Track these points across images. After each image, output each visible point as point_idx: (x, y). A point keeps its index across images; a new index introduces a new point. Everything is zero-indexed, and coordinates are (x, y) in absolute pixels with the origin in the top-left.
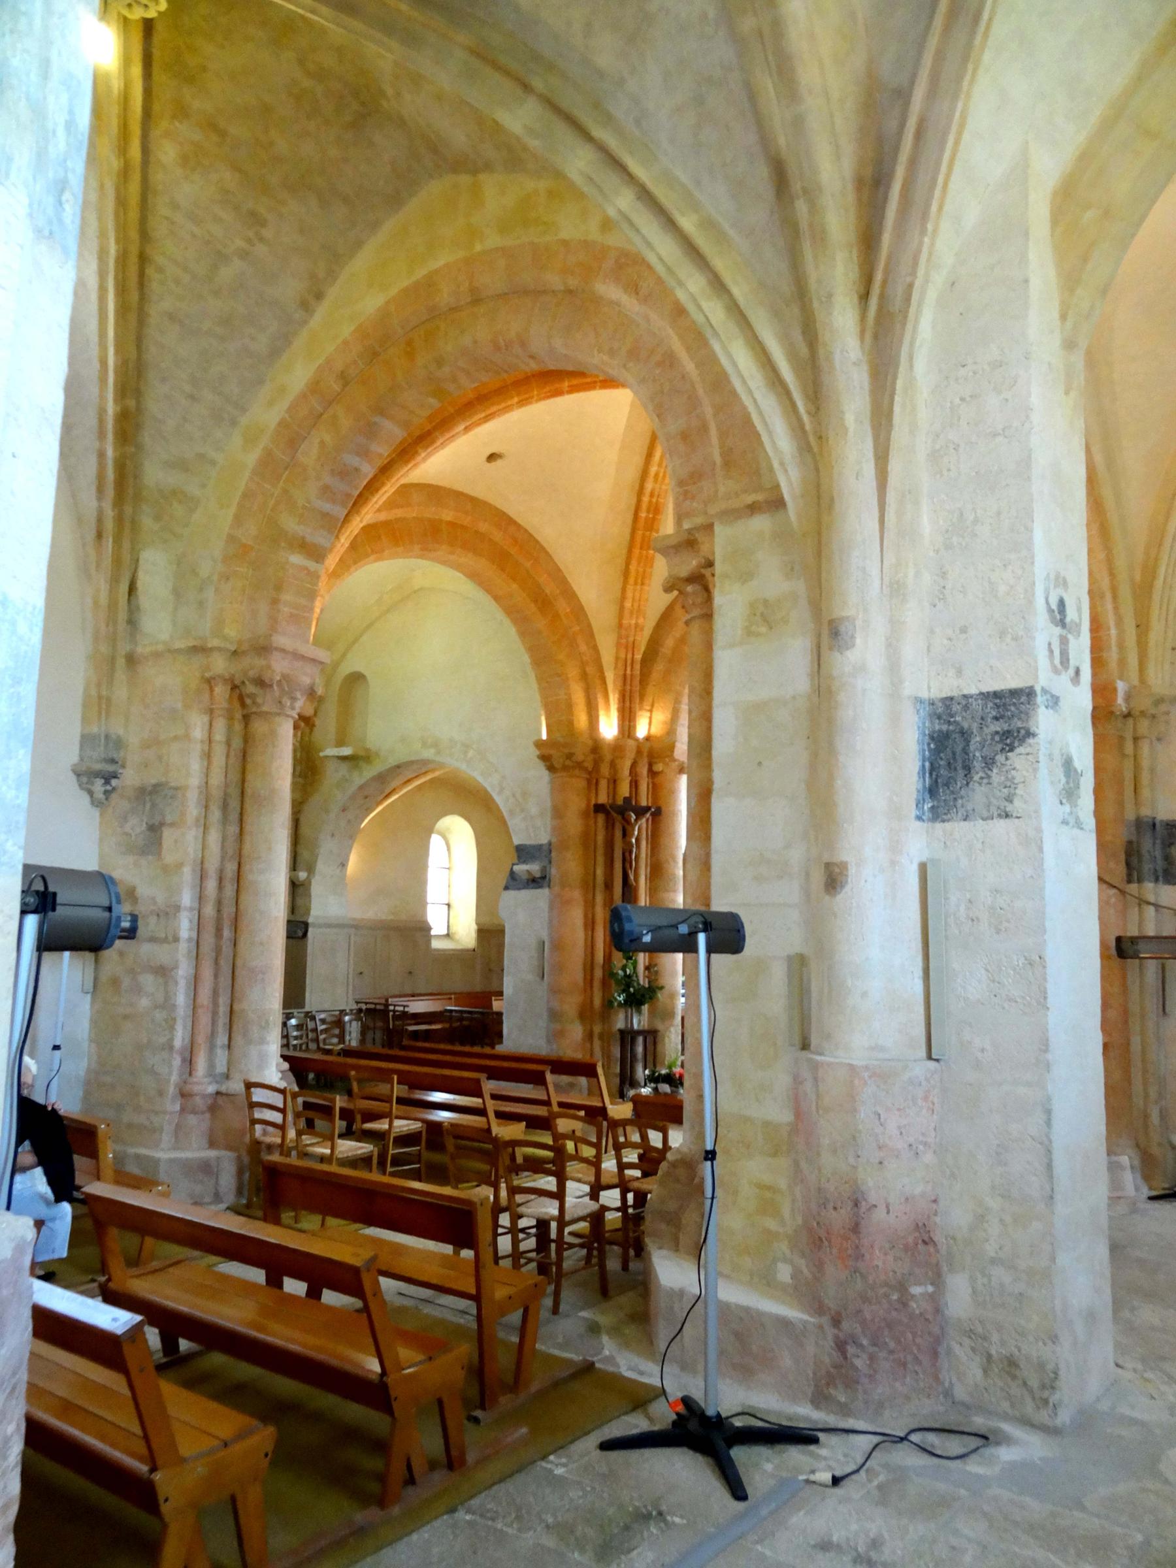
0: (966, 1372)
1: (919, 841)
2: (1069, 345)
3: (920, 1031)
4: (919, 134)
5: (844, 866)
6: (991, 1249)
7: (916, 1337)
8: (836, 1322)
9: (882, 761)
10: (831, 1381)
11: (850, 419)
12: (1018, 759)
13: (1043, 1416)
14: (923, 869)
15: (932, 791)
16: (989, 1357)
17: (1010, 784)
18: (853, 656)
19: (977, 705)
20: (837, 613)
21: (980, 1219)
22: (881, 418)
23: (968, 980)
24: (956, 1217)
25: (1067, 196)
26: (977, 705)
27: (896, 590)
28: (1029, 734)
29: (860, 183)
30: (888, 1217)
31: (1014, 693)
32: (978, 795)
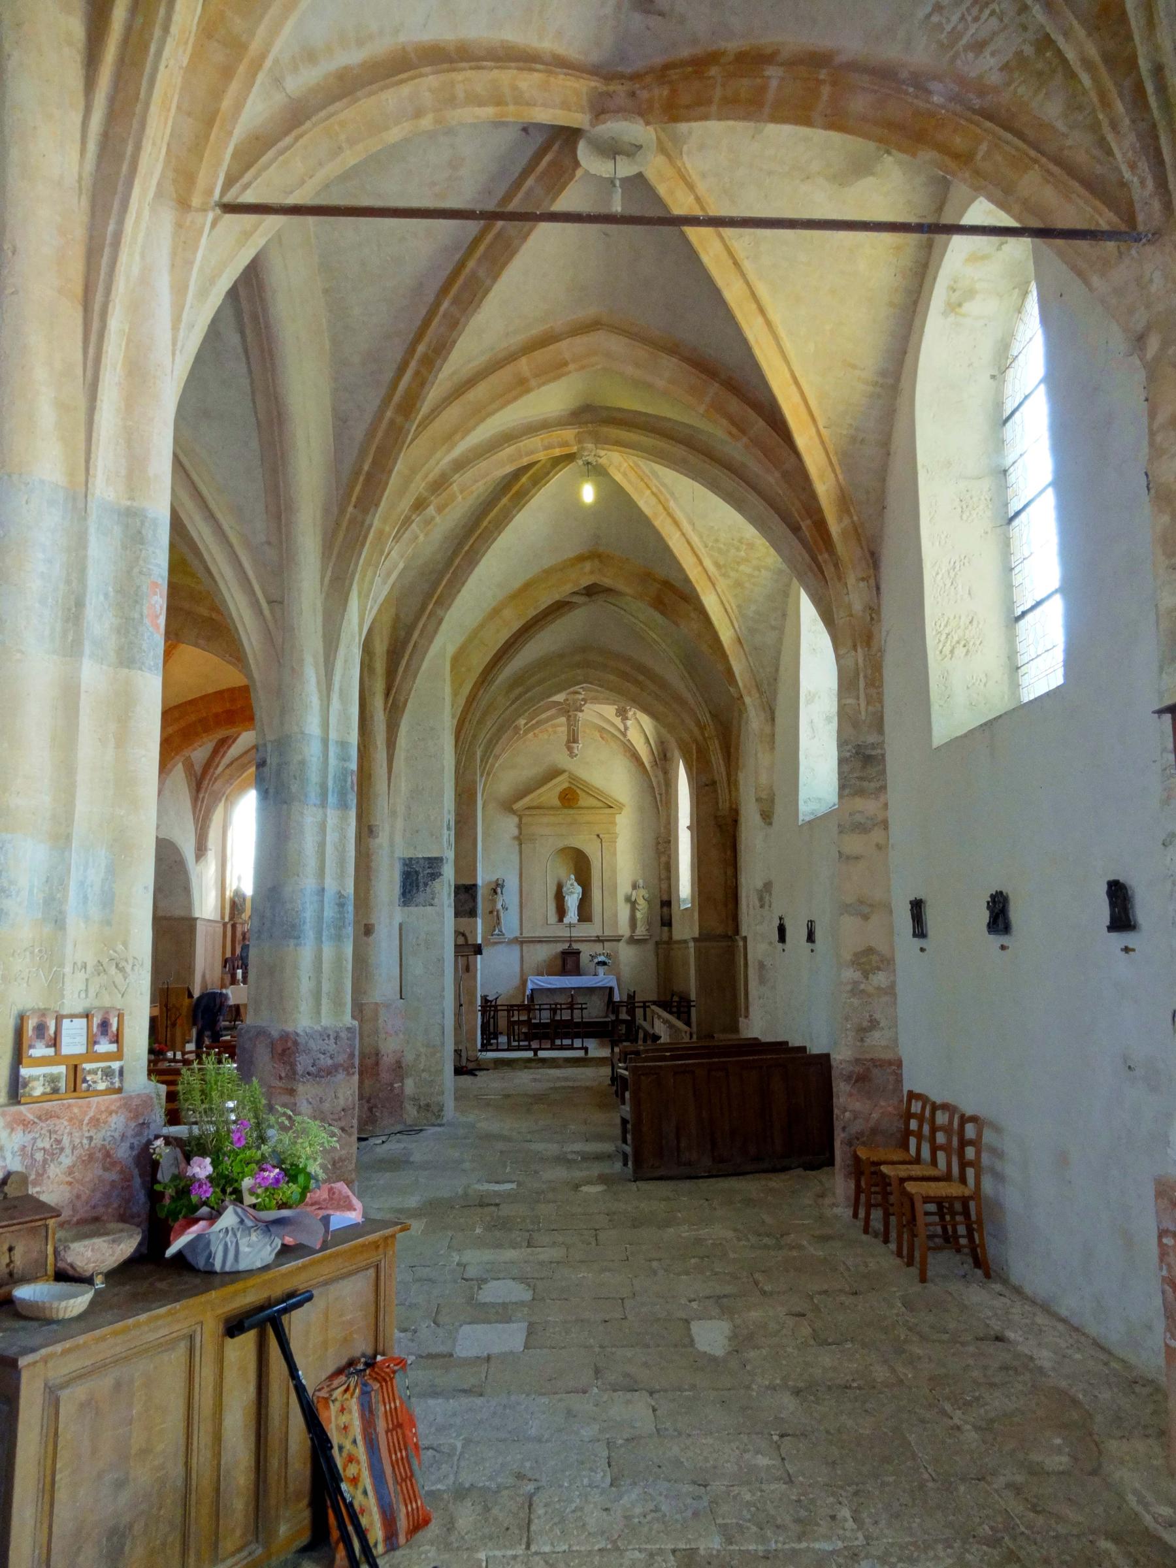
0: (411, 1112)
1: (399, 914)
2: (453, 717)
3: (398, 988)
4: (414, 646)
5: (373, 925)
6: (422, 1066)
7: (395, 1101)
8: (368, 1102)
9: (388, 882)
10: (366, 1123)
11: (379, 743)
12: (436, 884)
13: (439, 1121)
14: (401, 925)
15: (404, 894)
16: (420, 1107)
17: (433, 893)
18: (378, 841)
19: (421, 862)
20: (372, 823)
21: (418, 1056)
22: (391, 744)
23: (416, 968)
24: (409, 1057)
25: (456, 660)
26: (421, 862)
27: (393, 814)
28: (441, 875)
29: (388, 652)
30: (387, 1060)
31: (436, 858)
32: (421, 897)
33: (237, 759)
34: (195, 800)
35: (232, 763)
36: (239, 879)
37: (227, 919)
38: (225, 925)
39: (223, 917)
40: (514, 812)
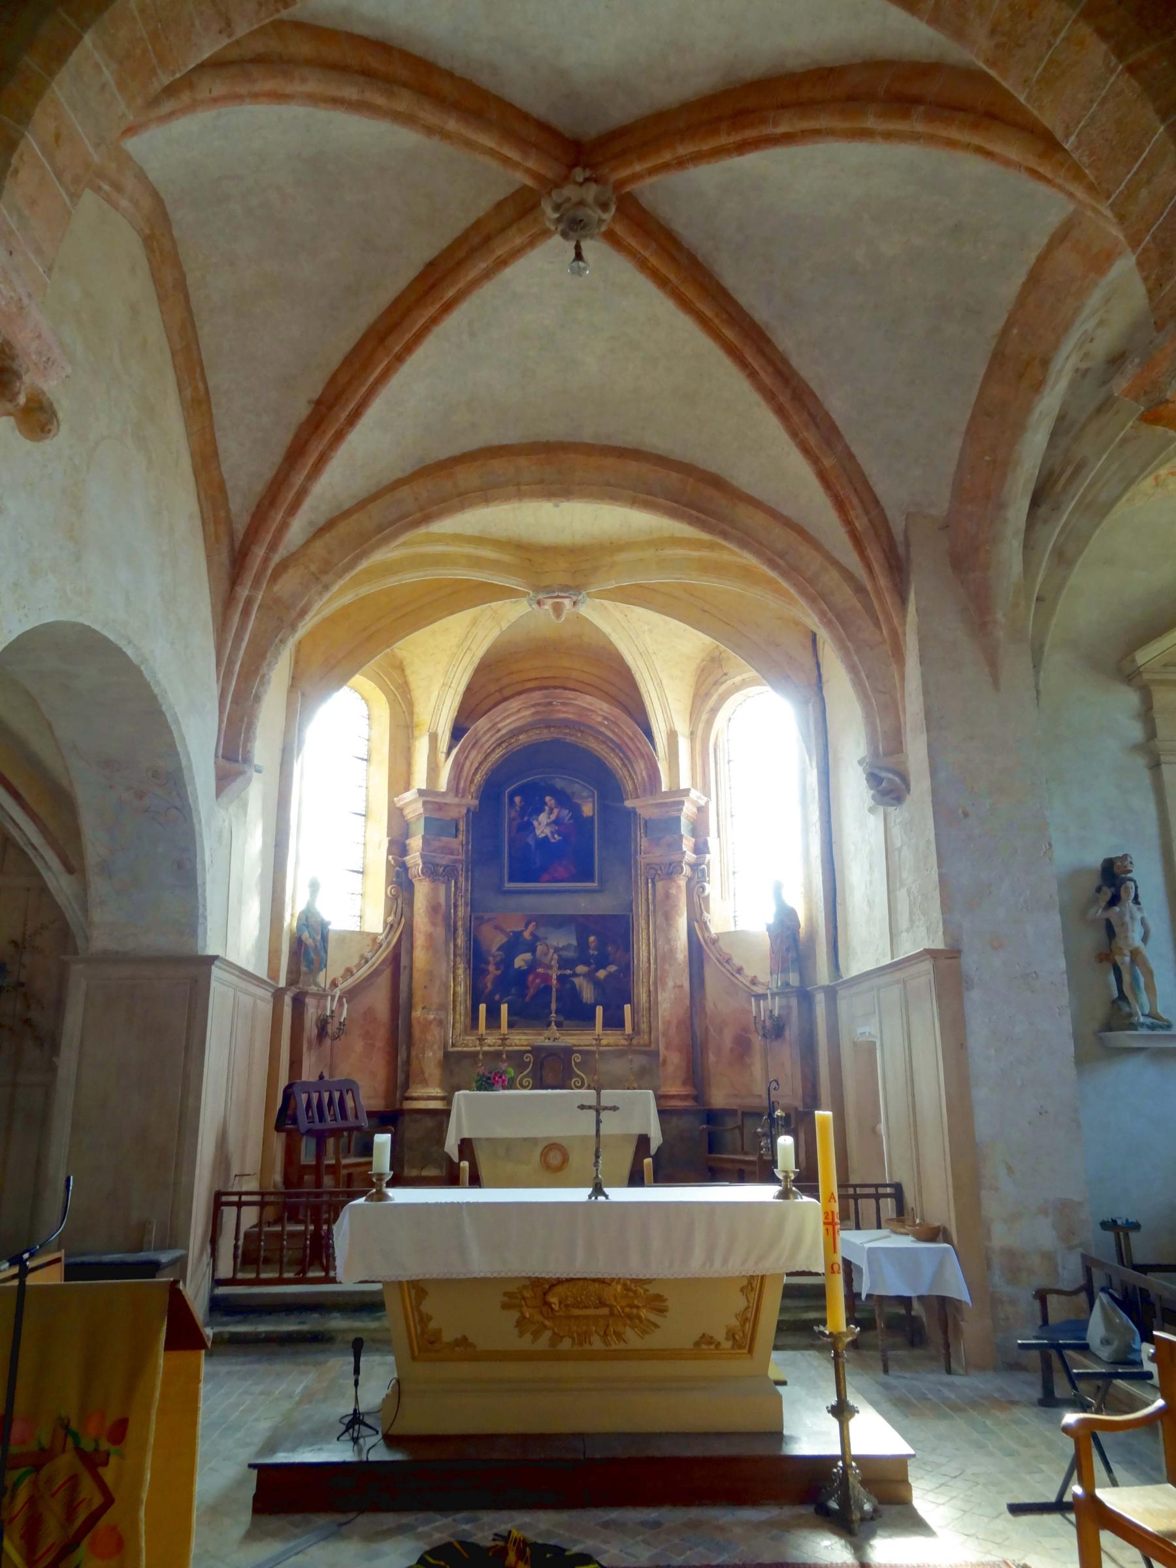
33: (346, 514)
34: (226, 603)
35: (329, 525)
36: (314, 887)
37: (282, 983)
38: (278, 995)
39: (273, 973)
40: (1129, 676)
